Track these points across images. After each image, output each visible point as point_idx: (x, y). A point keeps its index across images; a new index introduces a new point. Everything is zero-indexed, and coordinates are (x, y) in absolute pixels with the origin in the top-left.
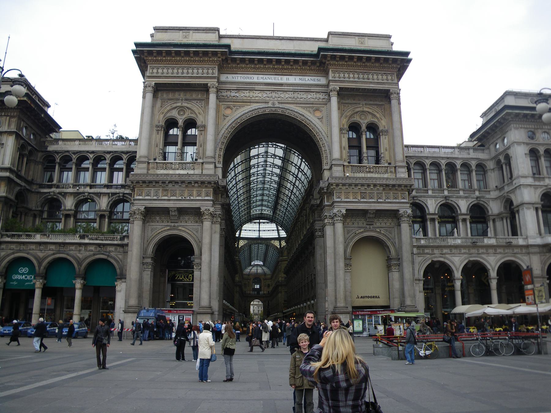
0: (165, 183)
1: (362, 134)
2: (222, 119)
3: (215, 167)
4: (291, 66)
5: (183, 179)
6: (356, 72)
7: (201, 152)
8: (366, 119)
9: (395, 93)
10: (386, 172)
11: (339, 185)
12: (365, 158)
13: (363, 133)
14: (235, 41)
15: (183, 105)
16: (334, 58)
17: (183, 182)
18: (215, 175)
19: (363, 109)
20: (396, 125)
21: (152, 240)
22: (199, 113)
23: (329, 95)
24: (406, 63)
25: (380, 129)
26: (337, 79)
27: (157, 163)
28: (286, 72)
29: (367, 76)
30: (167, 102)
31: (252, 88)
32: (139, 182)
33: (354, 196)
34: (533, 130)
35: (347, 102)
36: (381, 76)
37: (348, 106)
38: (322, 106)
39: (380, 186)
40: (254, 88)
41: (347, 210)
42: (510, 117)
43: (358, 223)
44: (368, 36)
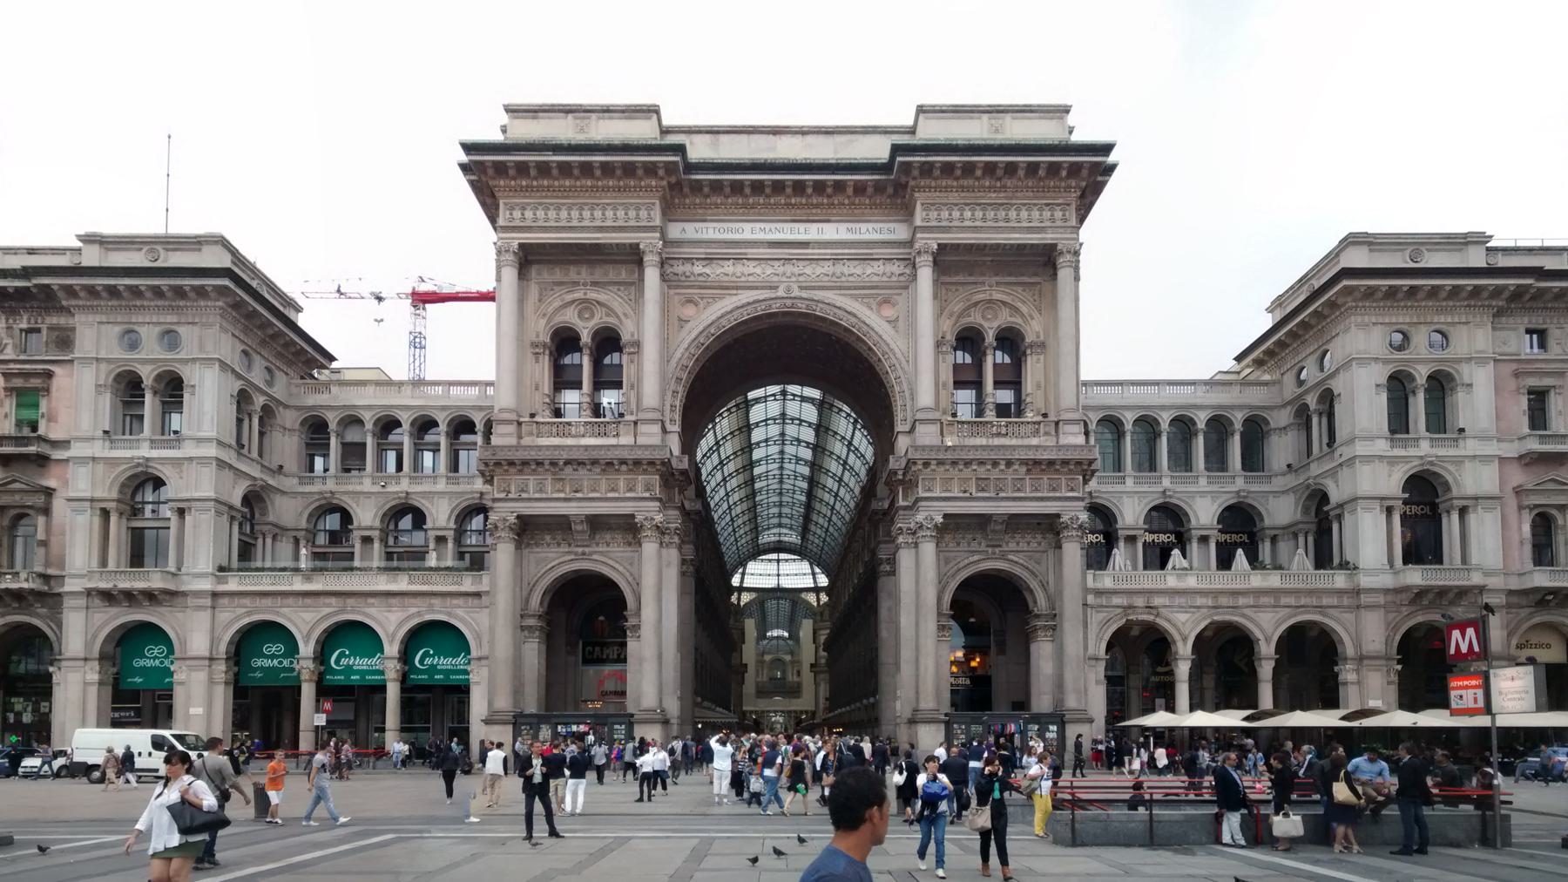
1: (985, 354)
3: (664, 431)
4: (829, 196)
8: (996, 317)
13: (988, 352)
14: (697, 138)
15: (588, 297)
18: (663, 446)
19: (991, 295)
21: (537, 581)
22: (625, 315)
23: (914, 267)
25: (1028, 340)
28: (816, 214)
30: (552, 290)
34: (1404, 327)
35: (955, 279)
37: (957, 290)
38: (896, 291)
40: (745, 254)
42: (1349, 299)
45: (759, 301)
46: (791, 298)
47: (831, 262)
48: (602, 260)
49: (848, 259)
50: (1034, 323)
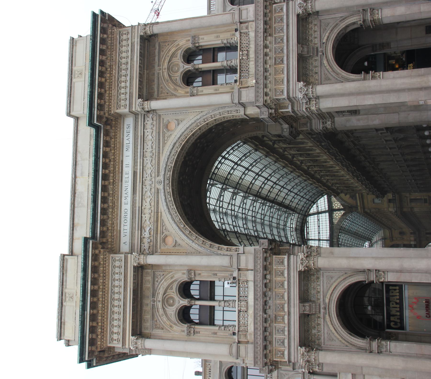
0: (266, 319)
1: (197, 69)
2: (180, 248)
5: (260, 294)
6: (118, 78)
7: (223, 275)
9: (145, 28)
10: (247, 34)
11: (266, 93)
12: (229, 63)
13: (197, 67)
15: (161, 300)
16: (101, 107)
17: (265, 294)
19: (165, 69)
20: (186, 25)
22: (172, 278)
23: (148, 112)
24: (105, 16)
25: (191, 46)
26: (128, 102)
27: (238, 331)
28: (119, 168)
29: (123, 65)
31: (139, 210)
32: (265, 355)
33: (279, 73)
35: (156, 89)
36: (123, 48)
37: (162, 88)
39: (266, 40)
40: (139, 207)
41: (299, 80)
43: (316, 67)
44: (72, 66)
45: (166, 199)
46: (164, 181)
47: (144, 159)
48: (141, 290)
49: (143, 150)
50: (181, 44)
